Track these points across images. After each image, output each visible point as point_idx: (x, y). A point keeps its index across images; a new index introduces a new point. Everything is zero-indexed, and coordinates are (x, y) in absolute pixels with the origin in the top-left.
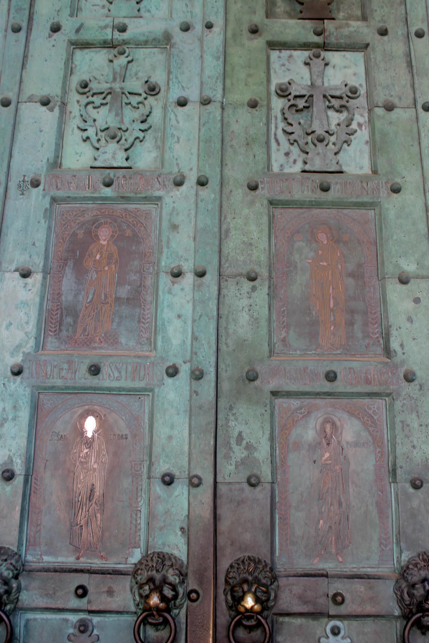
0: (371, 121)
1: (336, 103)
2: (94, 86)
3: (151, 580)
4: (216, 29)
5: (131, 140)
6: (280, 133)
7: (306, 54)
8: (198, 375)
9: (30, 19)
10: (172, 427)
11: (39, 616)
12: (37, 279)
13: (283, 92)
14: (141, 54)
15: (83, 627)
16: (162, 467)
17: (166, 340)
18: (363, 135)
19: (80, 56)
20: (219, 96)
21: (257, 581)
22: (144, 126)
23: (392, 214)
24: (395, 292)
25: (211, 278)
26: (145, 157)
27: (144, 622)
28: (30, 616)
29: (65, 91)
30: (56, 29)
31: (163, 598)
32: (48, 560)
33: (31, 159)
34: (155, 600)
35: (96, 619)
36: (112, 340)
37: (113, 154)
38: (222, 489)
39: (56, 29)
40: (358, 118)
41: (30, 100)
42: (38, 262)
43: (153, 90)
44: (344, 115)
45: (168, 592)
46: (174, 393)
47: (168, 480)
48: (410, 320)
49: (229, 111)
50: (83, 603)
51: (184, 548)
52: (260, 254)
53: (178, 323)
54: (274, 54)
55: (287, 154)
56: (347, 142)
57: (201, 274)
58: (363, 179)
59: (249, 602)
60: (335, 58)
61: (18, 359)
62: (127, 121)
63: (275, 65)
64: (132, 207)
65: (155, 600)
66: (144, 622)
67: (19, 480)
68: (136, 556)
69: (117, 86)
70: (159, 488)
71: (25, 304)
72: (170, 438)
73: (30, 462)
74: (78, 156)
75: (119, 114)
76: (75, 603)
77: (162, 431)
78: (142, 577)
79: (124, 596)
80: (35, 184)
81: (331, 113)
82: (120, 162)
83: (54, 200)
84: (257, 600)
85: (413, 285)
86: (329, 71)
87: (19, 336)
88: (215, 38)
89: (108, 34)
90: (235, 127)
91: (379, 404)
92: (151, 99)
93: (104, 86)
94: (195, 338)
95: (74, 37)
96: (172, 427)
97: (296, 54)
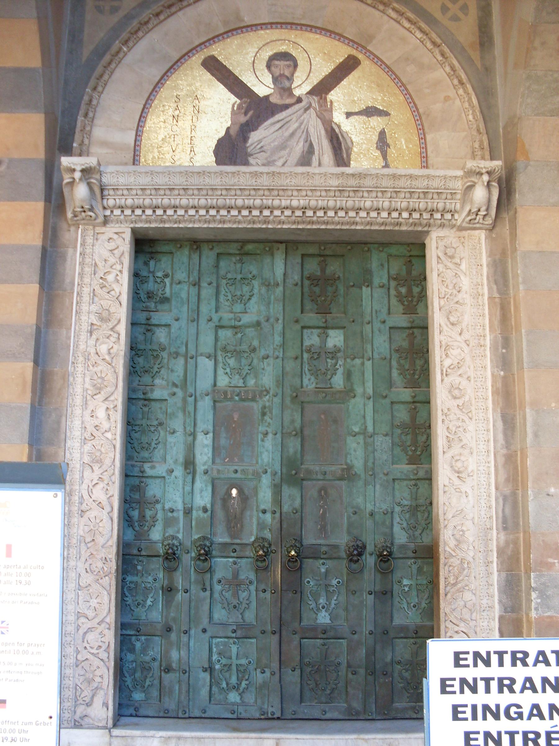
0: (344, 365)
1: (330, 356)
2: (228, 348)
3: (260, 545)
4: (280, 321)
5: (245, 374)
6: (306, 369)
7: (319, 330)
8: (274, 474)
9: (198, 315)
10: (265, 493)
11: (218, 559)
12: (211, 435)
13: (309, 351)
14: (248, 330)
15: (235, 563)
16: (262, 507)
17: (262, 460)
18: (340, 371)
19: (221, 333)
20: (281, 355)
21: (296, 546)
22: (250, 368)
23: (350, 407)
24: (349, 439)
25: (279, 436)
26: (251, 382)
27: (257, 560)
28: (216, 559)
29: (215, 350)
30: (210, 320)
31: (264, 552)
32: (221, 540)
33: (204, 382)
34: (261, 552)
35: (239, 560)
36: (241, 460)
37: (237, 381)
38: (284, 515)
39: (210, 320)
40: (340, 362)
41: (201, 355)
42: (211, 428)
43: (254, 350)
44: (334, 361)
45: (265, 550)
46: (266, 480)
47: (264, 512)
48: (355, 451)
49: (285, 361)
50: (235, 555)
51: (270, 535)
52: (298, 424)
53: (266, 453)
54: (305, 331)
55: (309, 380)
56: (336, 374)
57: (276, 434)
58: (340, 392)
59: (293, 553)
60: (331, 332)
61: (206, 467)
62: (242, 364)
63: (305, 337)
64: (246, 404)
65: (261, 552)
66: (257, 560)
67: (209, 512)
68: (253, 539)
69: (238, 349)
70: (261, 515)
71: (207, 446)
72: (264, 497)
73: (212, 505)
74: (223, 381)
75: (240, 362)
76: (232, 554)
77: (261, 495)
78: (256, 545)
79: (249, 552)
80: (207, 395)
81: (329, 360)
82: (241, 384)
83: (215, 402)
84: (296, 552)
85: (357, 437)
86: (329, 339)
87: (205, 458)
88: (279, 327)
89: (233, 323)
90: (288, 369)
91: (343, 483)
92: (252, 354)
93: (233, 348)
94: (273, 459)
95: (218, 324)
96: (265, 493)
97: (314, 331)
